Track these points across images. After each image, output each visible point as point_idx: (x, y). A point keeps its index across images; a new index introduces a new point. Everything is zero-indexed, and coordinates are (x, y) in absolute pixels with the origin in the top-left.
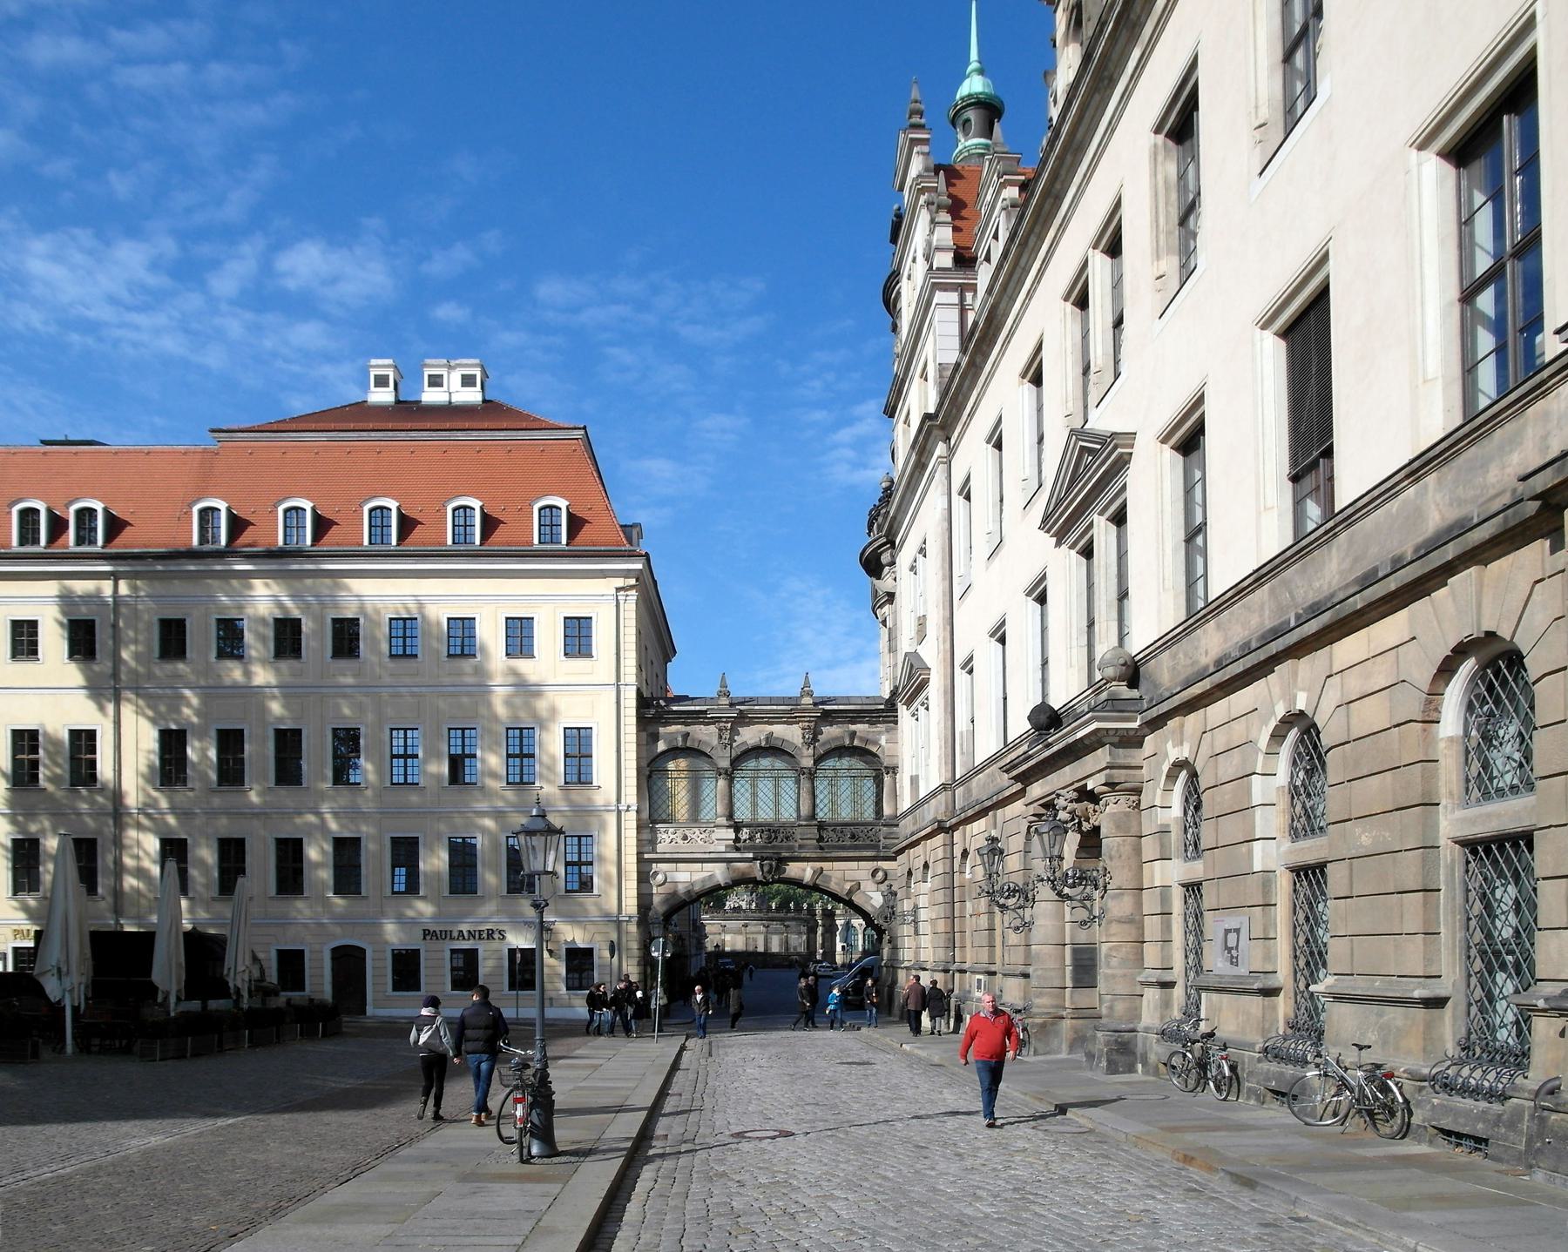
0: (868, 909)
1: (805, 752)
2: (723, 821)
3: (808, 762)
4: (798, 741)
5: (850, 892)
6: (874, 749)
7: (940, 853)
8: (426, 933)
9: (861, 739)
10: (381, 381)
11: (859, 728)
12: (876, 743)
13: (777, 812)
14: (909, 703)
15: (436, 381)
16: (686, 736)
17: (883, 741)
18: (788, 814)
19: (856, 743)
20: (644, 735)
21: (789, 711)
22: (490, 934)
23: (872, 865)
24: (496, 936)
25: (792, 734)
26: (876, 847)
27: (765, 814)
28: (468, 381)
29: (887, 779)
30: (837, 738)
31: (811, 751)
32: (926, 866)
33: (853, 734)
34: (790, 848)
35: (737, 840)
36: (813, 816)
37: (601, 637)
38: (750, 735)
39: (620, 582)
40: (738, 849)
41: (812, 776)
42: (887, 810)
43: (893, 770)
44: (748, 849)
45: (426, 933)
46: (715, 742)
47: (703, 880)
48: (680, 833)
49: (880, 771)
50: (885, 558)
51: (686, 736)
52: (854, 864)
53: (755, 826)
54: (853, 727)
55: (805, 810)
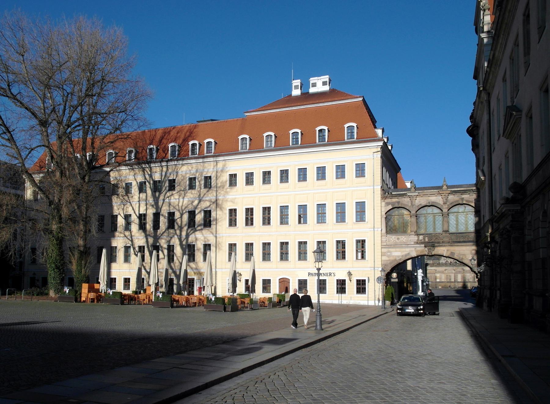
1: (444, 207)
3: (445, 210)
4: (441, 203)
8: (309, 274)
9: (467, 201)
10: (296, 87)
13: (434, 229)
15: (314, 85)
20: (383, 204)
22: (330, 274)
24: (332, 275)
28: (324, 83)
30: (457, 201)
31: (446, 206)
33: (463, 199)
35: (418, 239)
37: (368, 170)
39: (376, 150)
40: (417, 243)
44: (422, 243)
45: (309, 274)
46: (410, 205)
47: (406, 255)
51: (398, 202)
54: (463, 196)
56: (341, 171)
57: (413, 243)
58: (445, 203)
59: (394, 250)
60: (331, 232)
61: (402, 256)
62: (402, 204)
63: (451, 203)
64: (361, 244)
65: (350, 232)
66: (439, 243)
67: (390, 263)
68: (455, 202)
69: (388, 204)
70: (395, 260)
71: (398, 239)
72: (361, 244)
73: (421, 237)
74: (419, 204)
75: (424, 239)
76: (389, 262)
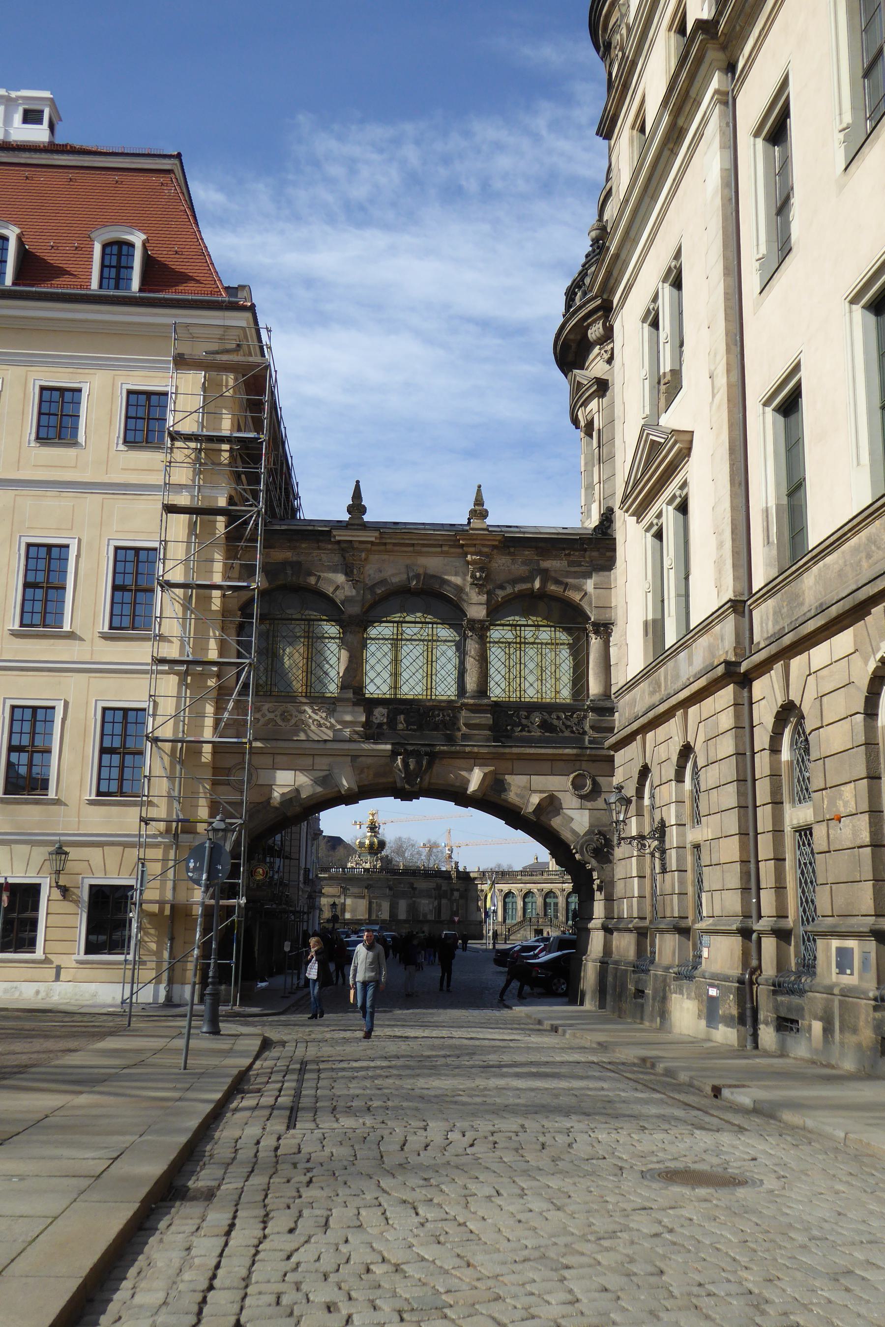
0: (566, 835)
2: (350, 695)
3: (477, 611)
7: (726, 720)
14: (639, 514)
18: (445, 689)
21: (452, 539)
27: (412, 687)
29: (595, 642)
32: (686, 751)
35: (367, 724)
36: (483, 690)
38: (390, 570)
41: (481, 629)
42: (594, 687)
43: (604, 629)
49: (583, 627)
50: (595, 331)
53: (397, 706)
55: (471, 683)
74: (378, 577)
75: (392, 722)
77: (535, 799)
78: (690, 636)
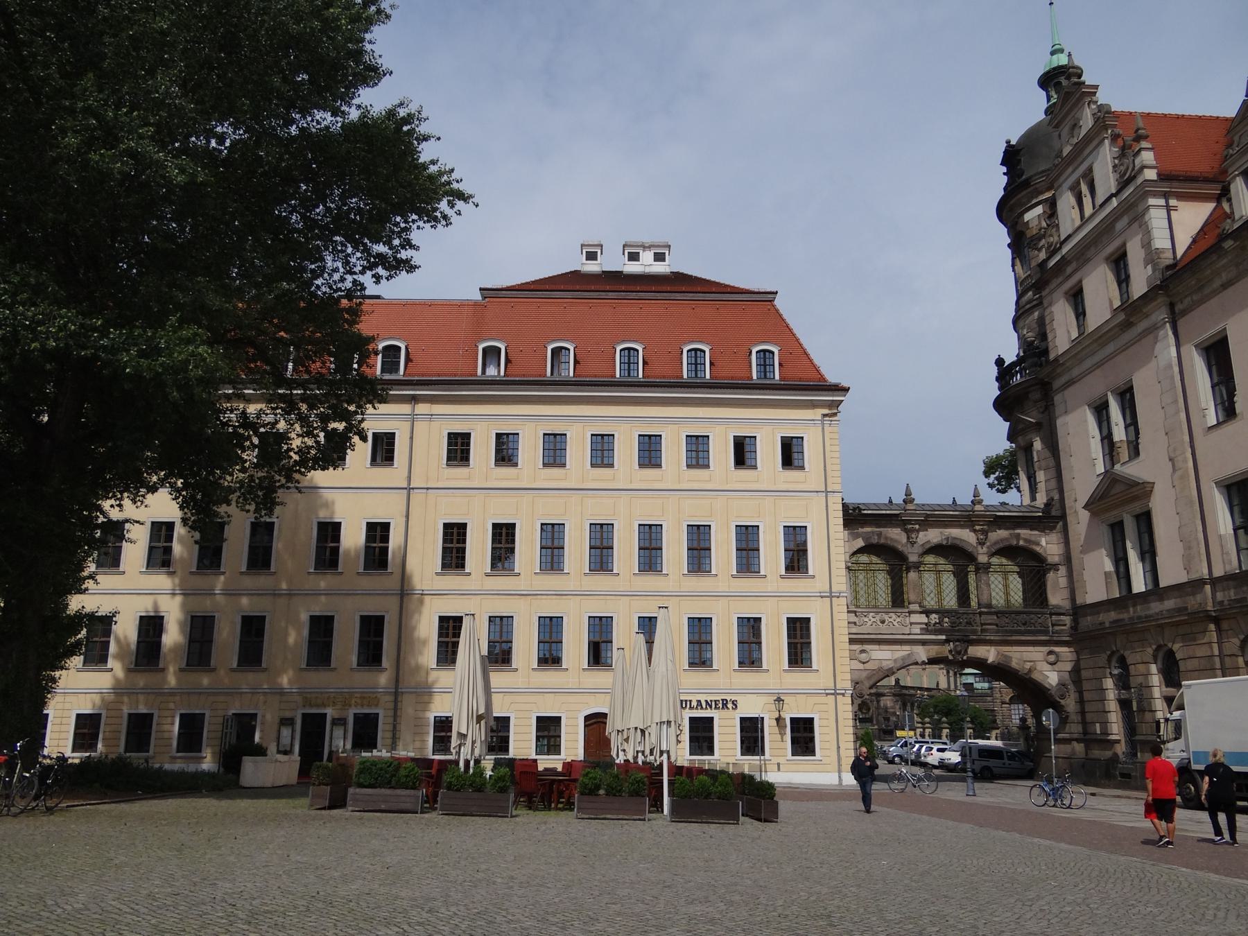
1: (981, 551)
5: (1030, 671)
6: (1037, 549)
9: (1026, 540)
11: (1024, 532)
12: (1038, 544)
16: (880, 534)
17: (1043, 542)
19: (1021, 543)
22: (725, 703)
23: (1046, 649)
24: (730, 705)
25: (966, 536)
26: (1046, 632)
30: (1006, 539)
31: (985, 549)
34: (974, 632)
46: (904, 540)
47: (903, 658)
48: (878, 617)
52: (1031, 649)
56: (743, 453)
57: (918, 631)
58: (982, 543)
59: (876, 647)
60: (724, 598)
61: (895, 661)
62: (886, 538)
63: (995, 543)
64: (799, 629)
65: (774, 599)
66: (974, 632)
67: (868, 678)
68: (1002, 540)
69: (855, 536)
70: (880, 669)
71: (883, 622)
72: (799, 629)
73: (934, 618)
76: (864, 674)
77: (1028, 666)
78: (1156, 591)
